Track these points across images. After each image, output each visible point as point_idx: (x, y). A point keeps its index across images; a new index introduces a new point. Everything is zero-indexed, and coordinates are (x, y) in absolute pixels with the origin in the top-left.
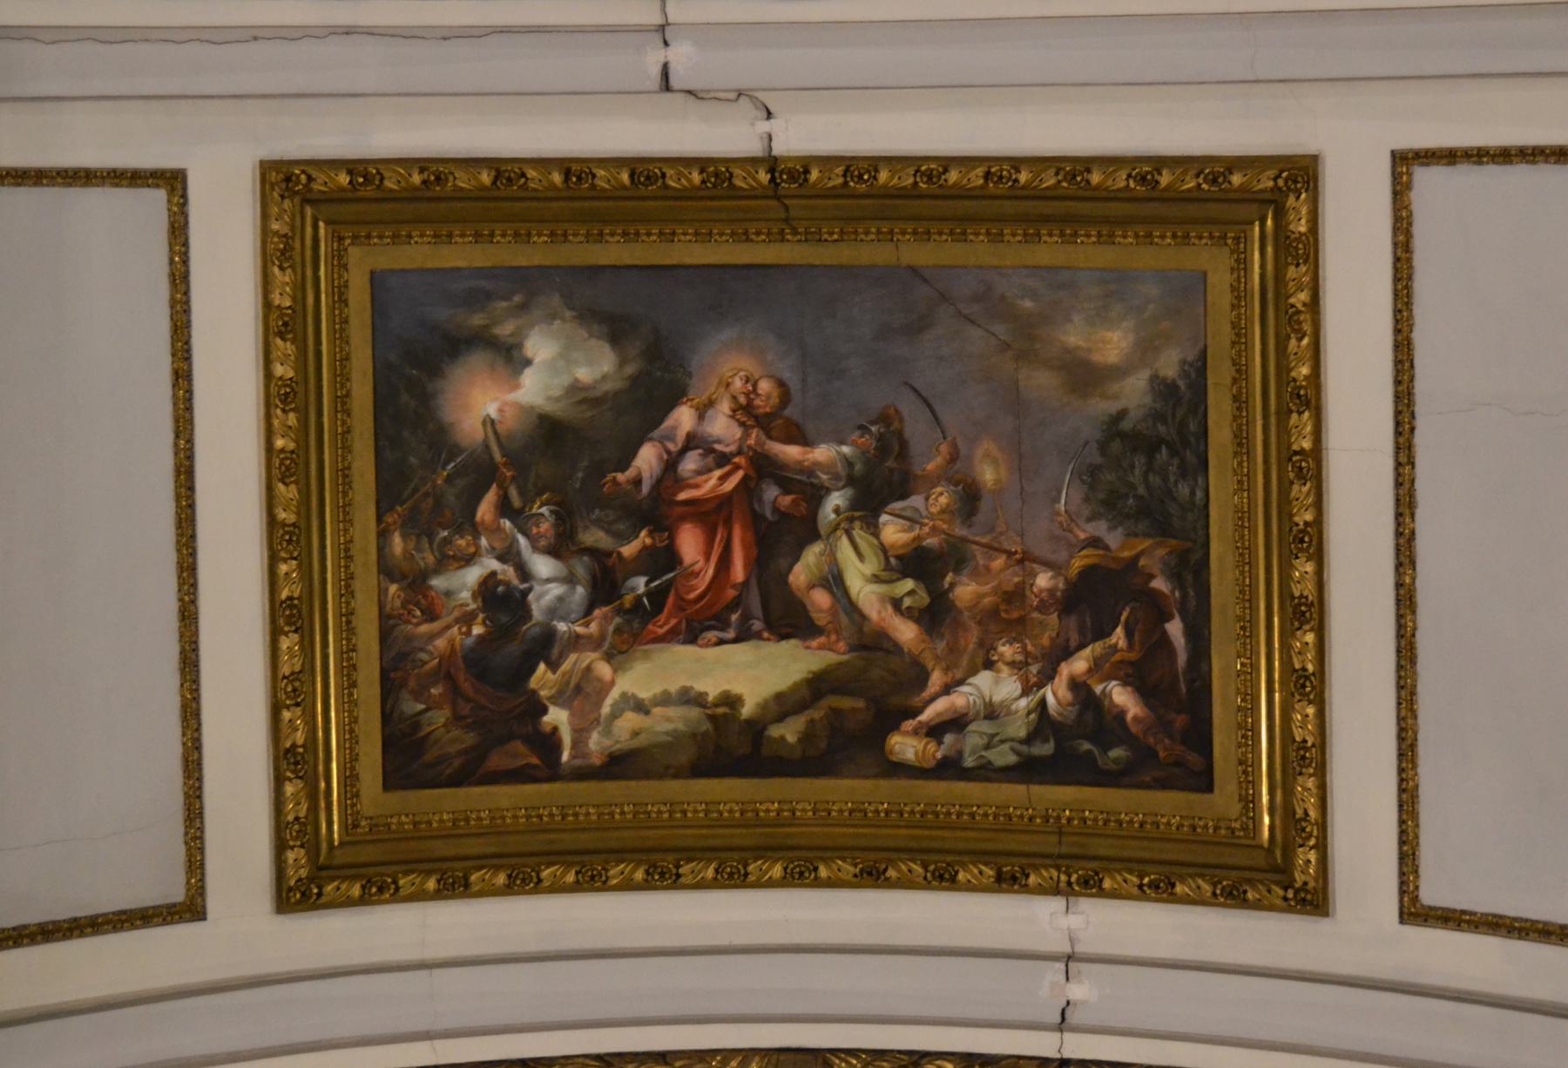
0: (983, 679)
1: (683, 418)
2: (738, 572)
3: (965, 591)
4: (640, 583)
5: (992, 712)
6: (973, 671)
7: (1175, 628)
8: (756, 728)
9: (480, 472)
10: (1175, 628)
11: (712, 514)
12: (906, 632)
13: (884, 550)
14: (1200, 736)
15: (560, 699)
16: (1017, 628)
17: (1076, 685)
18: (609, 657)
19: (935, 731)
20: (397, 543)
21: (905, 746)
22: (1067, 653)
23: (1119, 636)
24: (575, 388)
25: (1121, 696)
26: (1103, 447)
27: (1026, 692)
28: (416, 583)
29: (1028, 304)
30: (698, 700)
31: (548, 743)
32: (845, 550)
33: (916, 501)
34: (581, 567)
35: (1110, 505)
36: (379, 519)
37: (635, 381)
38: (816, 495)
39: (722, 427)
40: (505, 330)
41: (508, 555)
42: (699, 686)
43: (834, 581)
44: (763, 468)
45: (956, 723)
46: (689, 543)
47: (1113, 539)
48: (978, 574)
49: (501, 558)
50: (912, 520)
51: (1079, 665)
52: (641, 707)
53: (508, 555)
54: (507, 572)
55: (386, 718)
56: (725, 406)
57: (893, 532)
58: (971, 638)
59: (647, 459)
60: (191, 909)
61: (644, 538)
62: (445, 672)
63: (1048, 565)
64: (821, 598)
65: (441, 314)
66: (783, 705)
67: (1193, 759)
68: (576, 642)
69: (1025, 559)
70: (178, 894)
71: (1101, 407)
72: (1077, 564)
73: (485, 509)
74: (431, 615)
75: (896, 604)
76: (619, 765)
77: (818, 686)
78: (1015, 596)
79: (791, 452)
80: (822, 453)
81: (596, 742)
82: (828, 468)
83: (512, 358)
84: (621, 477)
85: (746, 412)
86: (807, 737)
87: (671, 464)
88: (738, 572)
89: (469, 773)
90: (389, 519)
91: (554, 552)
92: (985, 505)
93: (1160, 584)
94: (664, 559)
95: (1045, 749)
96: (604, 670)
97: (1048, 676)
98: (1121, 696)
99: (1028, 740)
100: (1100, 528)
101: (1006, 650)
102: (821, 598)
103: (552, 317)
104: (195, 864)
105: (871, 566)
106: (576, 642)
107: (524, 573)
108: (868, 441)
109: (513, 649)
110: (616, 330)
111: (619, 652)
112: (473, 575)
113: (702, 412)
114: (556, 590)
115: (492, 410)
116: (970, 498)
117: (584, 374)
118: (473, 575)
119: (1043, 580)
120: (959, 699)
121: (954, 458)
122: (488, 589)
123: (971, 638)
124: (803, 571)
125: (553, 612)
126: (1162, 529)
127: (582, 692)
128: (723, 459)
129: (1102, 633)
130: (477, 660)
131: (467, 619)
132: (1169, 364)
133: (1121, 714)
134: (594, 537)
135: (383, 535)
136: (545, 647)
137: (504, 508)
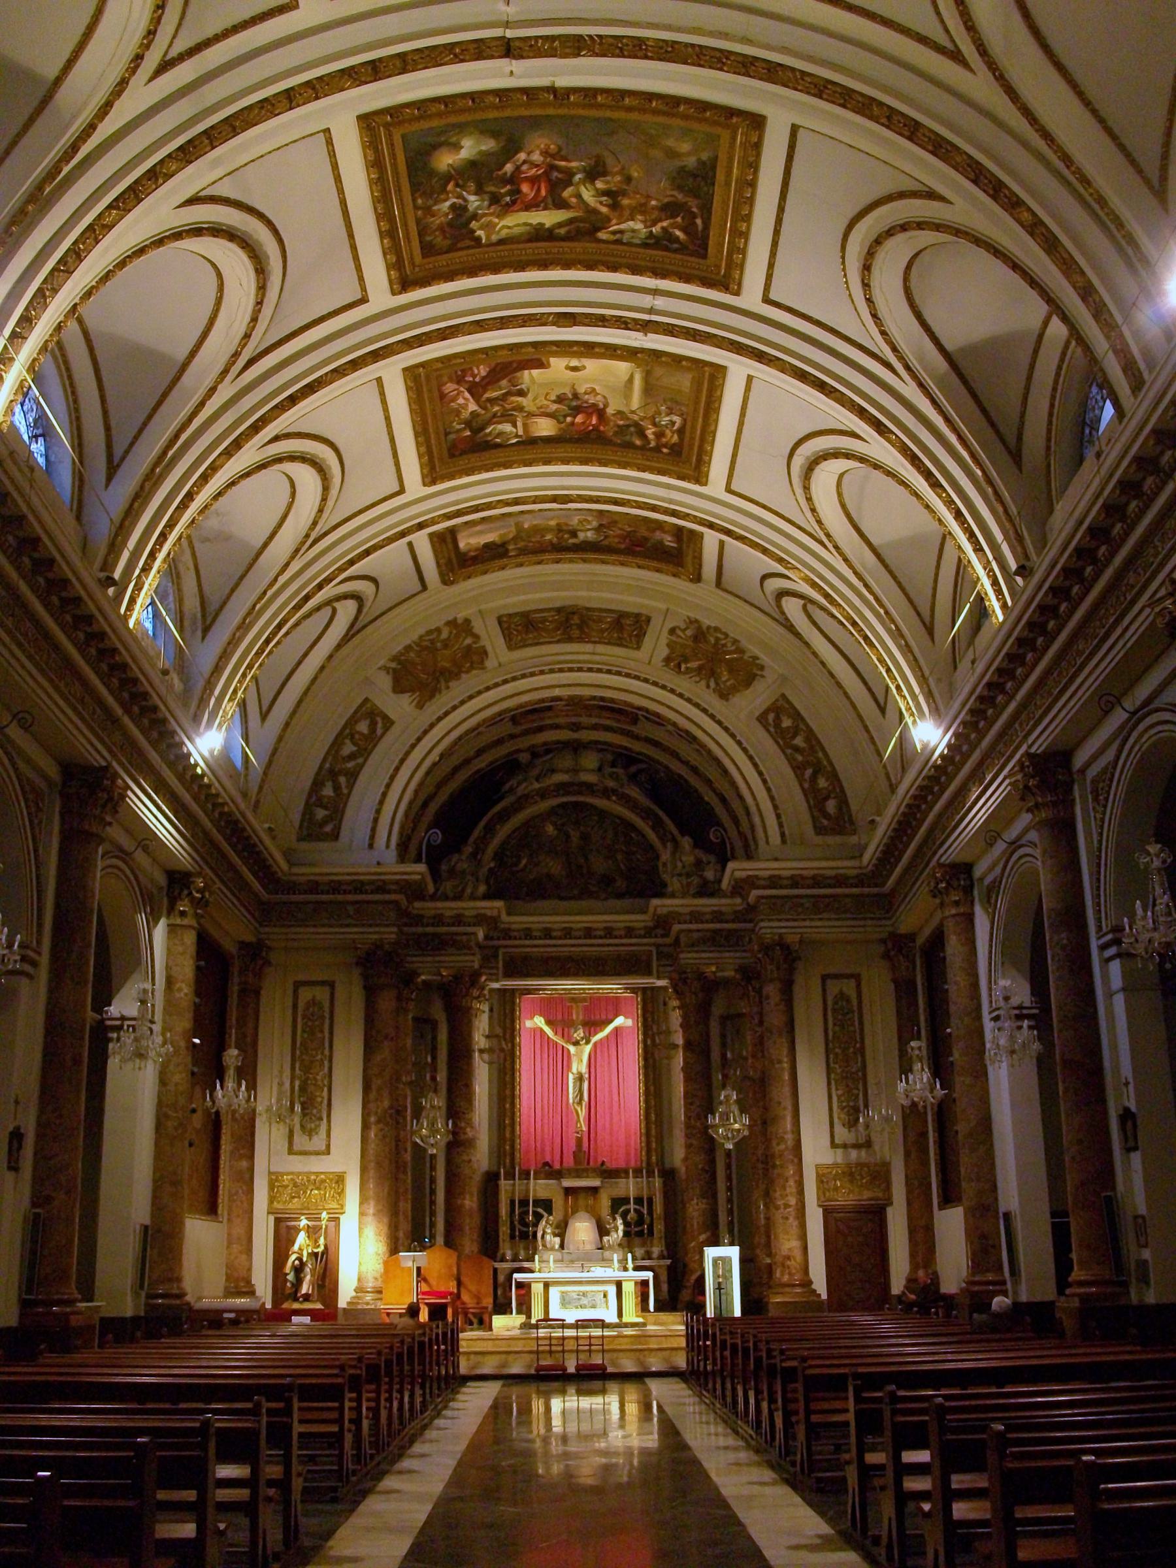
0: (631, 223)
1: (522, 156)
2: (543, 193)
3: (625, 202)
4: (508, 199)
5: (633, 231)
6: (628, 220)
7: (699, 221)
8: (550, 231)
9: (447, 178)
10: (699, 221)
11: (533, 181)
12: (604, 210)
13: (597, 190)
14: (704, 246)
15: (481, 228)
16: (643, 213)
17: (663, 228)
18: (498, 217)
19: (614, 233)
20: (420, 201)
21: (602, 235)
22: (661, 220)
23: (679, 219)
24: (481, 153)
25: (678, 233)
26: (678, 173)
27: (646, 227)
28: (428, 210)
29: (653, 132)
30: (530, 225)
31: (479, 239)
32: (583, 190)
33: (609, 178)
34: (486, 197)
35: (680, 188)
36: (412, 195)
37: (503, 147)
38: (573, 174)
39: (536, 157)
40: (454, 139)
41: (460, 196)
42: (530, 221)
43: (579, 196)
44: (552, 167)
45: (621, 232)
46: (525, 188)
47: (680, 197)
48: (630, 198)
49: (457, 198)
50: (607, 182)
51: (665, 224)
52: (509, 227)
53: (460, 196)
54: (460, 201)
55: (421, 242)
56: (538, 152)
57: (600, 185)
58: (627, 213)
59: (509, 168)
60: (364, 300)
61: (508, 187)
62: (441, 228)
63: (657, 200)
64: (574, 200)
65: (430, 140)
66: (560, 225)
67: (702, 252)
68: (485, 215)
69: (649, 197)
70: (360, 297)
71: (678, 163)
72: (666, 200)
73: (450, 187)
74: (433, 216)
75: (601, 203)
76: (501, 242)
77: (571, 221)
78: (642, 205)
79: (563, 163)
80: (574, 164)
81: (494, 238)
82: (577, 168)
83: (457, 147)
84: (500, 173)
85: (545, 153)
86: (569, 232)
87: (518, 168)
88: (543, 193)
89: (452, 249)
90: (417, 195)
91: (476, 194)
92: (634, 182)
93: (695, 210)
94: (519, 191)
95: (652, 241)
96: (496, 220)
97: (654, 224)
98: (678, 233)
99: (647, 238)
100: (675, 193)
101: (640, 217)
102: (574, 200)
103: (471, 133)
104: (364, 289)
105: (592, 193)
106: (485, 215)
107: (465, 200)
108: (592, 162)
109: (463, 220)
110: (495, 135)
111: (500, 216)
112: (448, 204)
113: (529, 154)
114: (477, 203)
115: (450, 162)
116: (629, 179)
117: (483, 148)
118: (448, 204)
119: (653, 203)
120: (622, 226)
121: (623, 168)
122: (453, 207)
123: (627, 213)
124: (566, 194)
125: (478, 208)
126: (697, 196)
127: (489, 227)
128: (537, 166)
129: (673, 216)
130: (450, 224)
131: (447, 214)
132: (705, 156)
133: (678, 238)
134: (492, 189)
135: (414, 200)
136: (475, 217)
137: (457, 185)
